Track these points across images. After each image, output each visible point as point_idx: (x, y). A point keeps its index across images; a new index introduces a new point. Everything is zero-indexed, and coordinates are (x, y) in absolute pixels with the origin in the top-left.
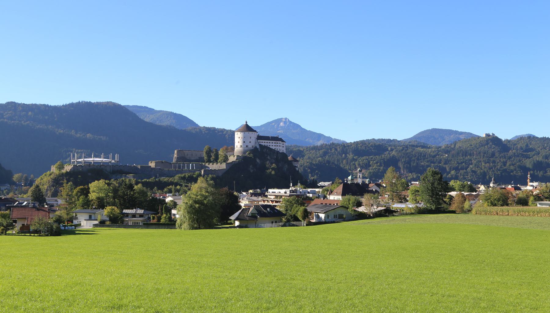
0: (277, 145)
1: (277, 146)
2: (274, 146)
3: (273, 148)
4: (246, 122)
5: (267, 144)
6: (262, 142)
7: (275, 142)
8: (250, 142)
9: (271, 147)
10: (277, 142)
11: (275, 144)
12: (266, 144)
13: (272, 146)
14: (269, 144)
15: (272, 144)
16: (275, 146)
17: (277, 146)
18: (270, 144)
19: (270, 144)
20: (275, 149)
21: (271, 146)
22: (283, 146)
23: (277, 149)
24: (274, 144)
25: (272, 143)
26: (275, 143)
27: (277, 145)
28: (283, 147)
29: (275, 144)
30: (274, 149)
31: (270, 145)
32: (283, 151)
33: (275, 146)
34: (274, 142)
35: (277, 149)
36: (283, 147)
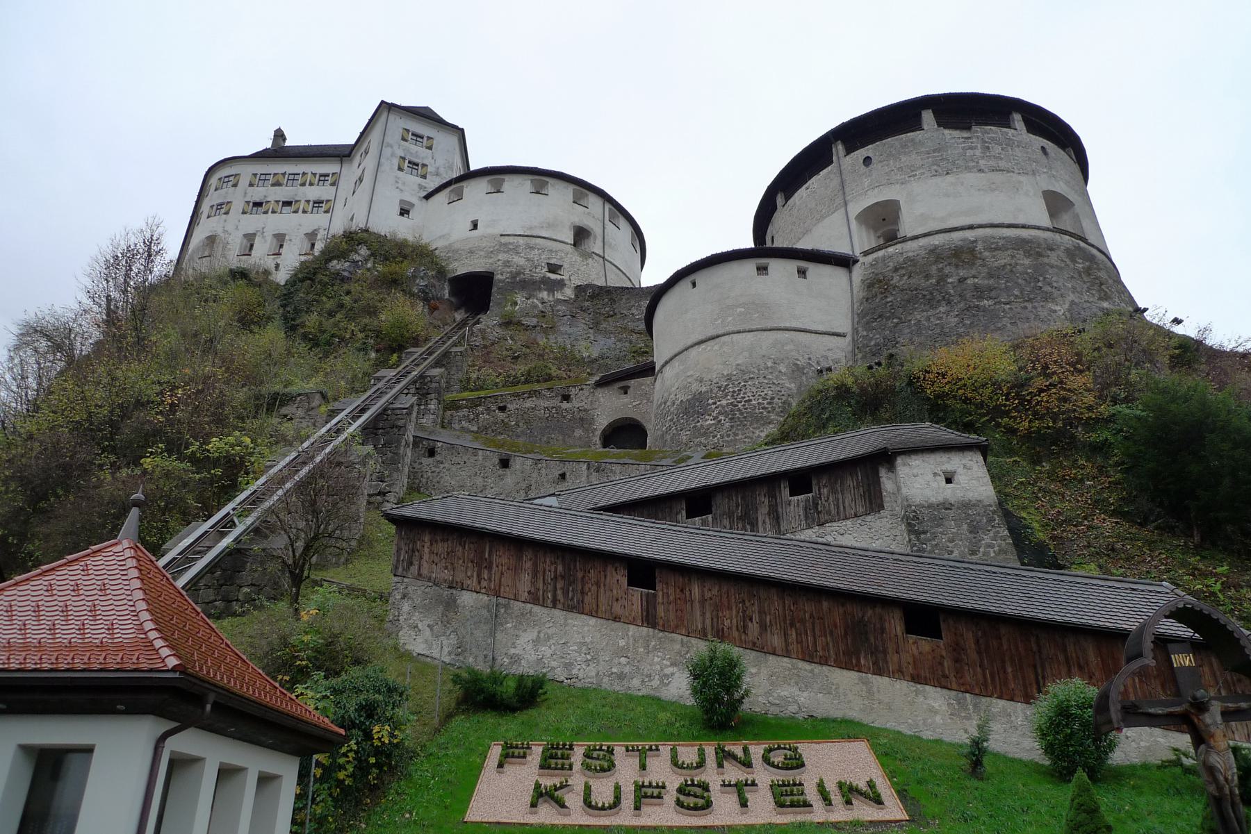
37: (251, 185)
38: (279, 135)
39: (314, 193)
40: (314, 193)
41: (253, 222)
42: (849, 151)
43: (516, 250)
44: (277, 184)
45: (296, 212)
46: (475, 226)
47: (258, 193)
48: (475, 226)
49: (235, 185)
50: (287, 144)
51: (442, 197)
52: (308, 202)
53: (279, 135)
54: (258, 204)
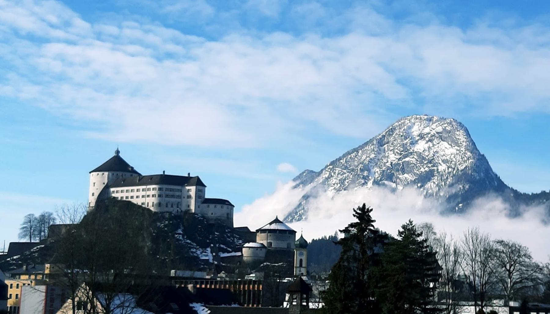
0: (148, 193)
1: (148, 196)
2: (141, 197)
4: (118, 152)
5: (127, 194)
6: (117, 192)
7: (144, 187)
9: (134, 201)
10: (148, 187)
11: (144, 193)
12: (124, 195)
13: (137, 197)
14: (130, 194)
16: (143, 196)
17: (148, 196)
20: (143, 204)
21: (135, 197)
23: (148, 203)
24: (141, 193)
25: (138, 190)
26: (143, 190)
27: (148, 193)
29: (144, 193)
30: (140, 204)
31: (132, 197)
33: (143, 196)
34: (141, 188)
35: (148, 203)
37: (166, 190)
38: (164, 172)
39: (177, 194)
40: (177, 194)
41: (167, 199)
42: (269, 233)
43: (219, 220)
44: (170, 191)
45: (175, 198)
46: (212, 214)
47: (167, 192)
48: (212, 214)
49: (163, 190)
50: (166, 173)
51: (205, 205)
52: (177, 196)
53: (164, 172)
54: (167, 196)
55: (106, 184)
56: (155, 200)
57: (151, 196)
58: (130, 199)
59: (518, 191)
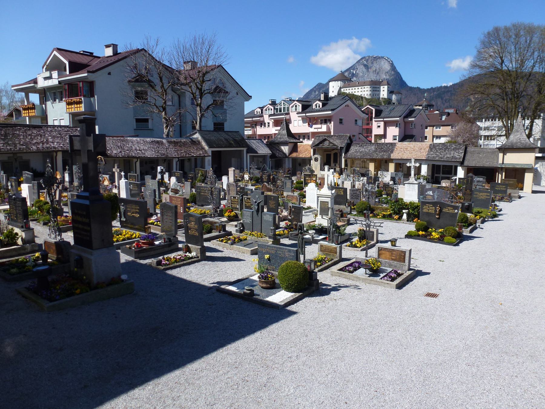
0: (364, 89)
1: (364, 91)
3: (359, 94)
5: (352, 91)
8: (333, 92)
9: (356, 94)
11: (362, 90)
15: (358, 90)
17: (364, 91)
18: (355, 90)
19: (355, 90)
21: (356, 92)
22: (383, 89)
25: (358, 89)
26: (361, 88)
28: (383, 91)
30: (359, 95)
32: (383, 95)
33: (361, 91)
34: (360, 87)
36: (383, 91)
55: (339, 87)
56: (369, 93)
57: (366, 91)
58: (353, 93)
59: (434, 87)
